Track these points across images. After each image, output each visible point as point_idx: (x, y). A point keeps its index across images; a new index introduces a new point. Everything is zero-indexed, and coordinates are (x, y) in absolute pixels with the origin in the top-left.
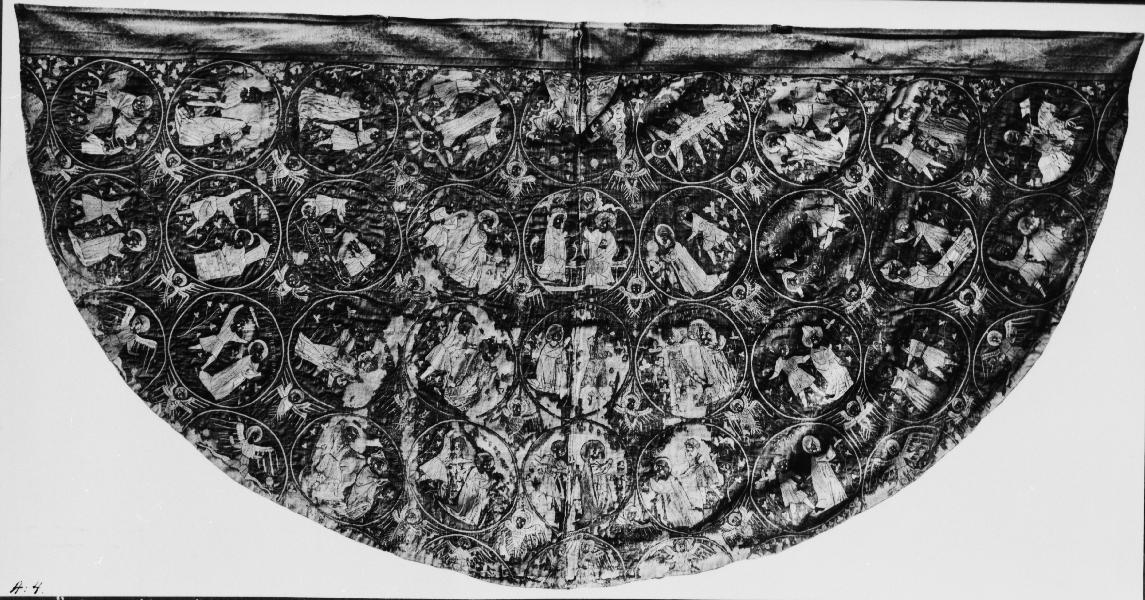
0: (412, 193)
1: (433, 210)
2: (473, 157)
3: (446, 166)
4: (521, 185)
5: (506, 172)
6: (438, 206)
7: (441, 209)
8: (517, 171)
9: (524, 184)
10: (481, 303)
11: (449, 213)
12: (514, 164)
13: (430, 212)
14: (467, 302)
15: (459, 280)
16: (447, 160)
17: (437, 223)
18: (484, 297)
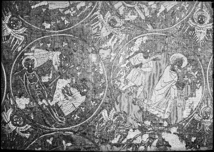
0: (115, 42)
1: (133, 55)
2: (166, 9)
3: (143, 18)
4: (205, 32)
5: (194, 21)
6: (137, 53)
7: (139, 54)
8: (202, 19)
9: (207, 30)
10: (174, 130)
11: (145, 58)
12: (200, 13)
13: (130, 57)
14: (162, 131)
15: (155, 113)
16: (144, 13)
17: (137, 66)
18: (176, 125)
